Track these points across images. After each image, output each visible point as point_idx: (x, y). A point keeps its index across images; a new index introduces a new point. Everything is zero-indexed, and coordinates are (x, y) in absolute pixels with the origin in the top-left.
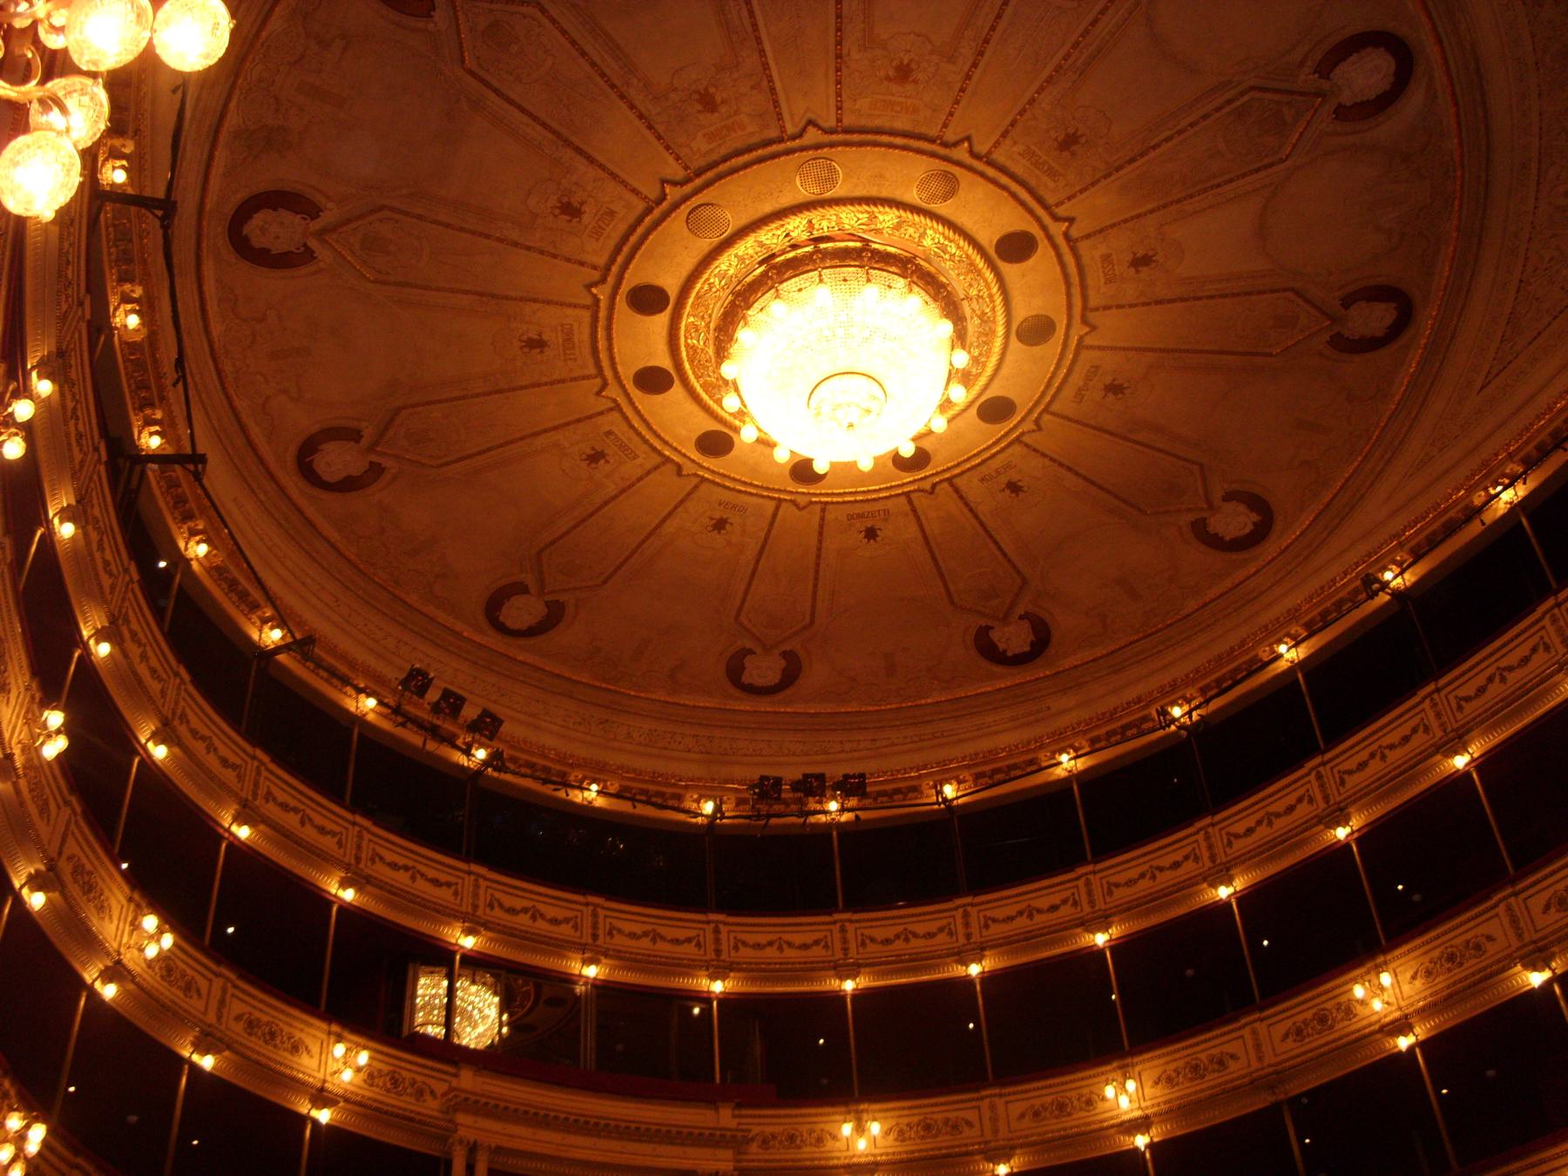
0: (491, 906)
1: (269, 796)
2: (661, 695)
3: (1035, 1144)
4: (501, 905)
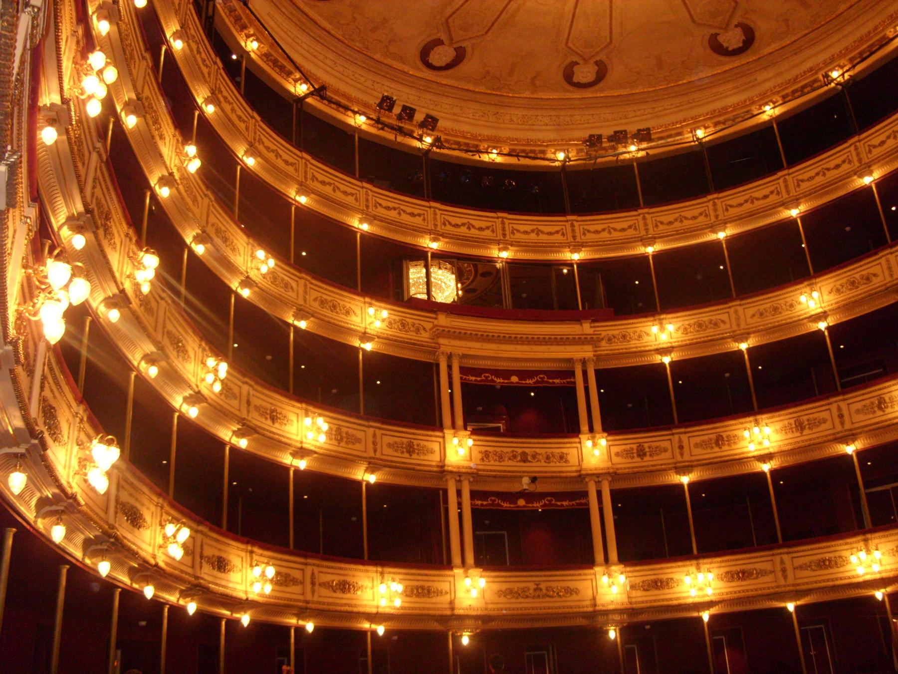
0: (445, 224)
1: (314, 178)
2: (527, 94)
3: (762, 330)
4: (450, 223)
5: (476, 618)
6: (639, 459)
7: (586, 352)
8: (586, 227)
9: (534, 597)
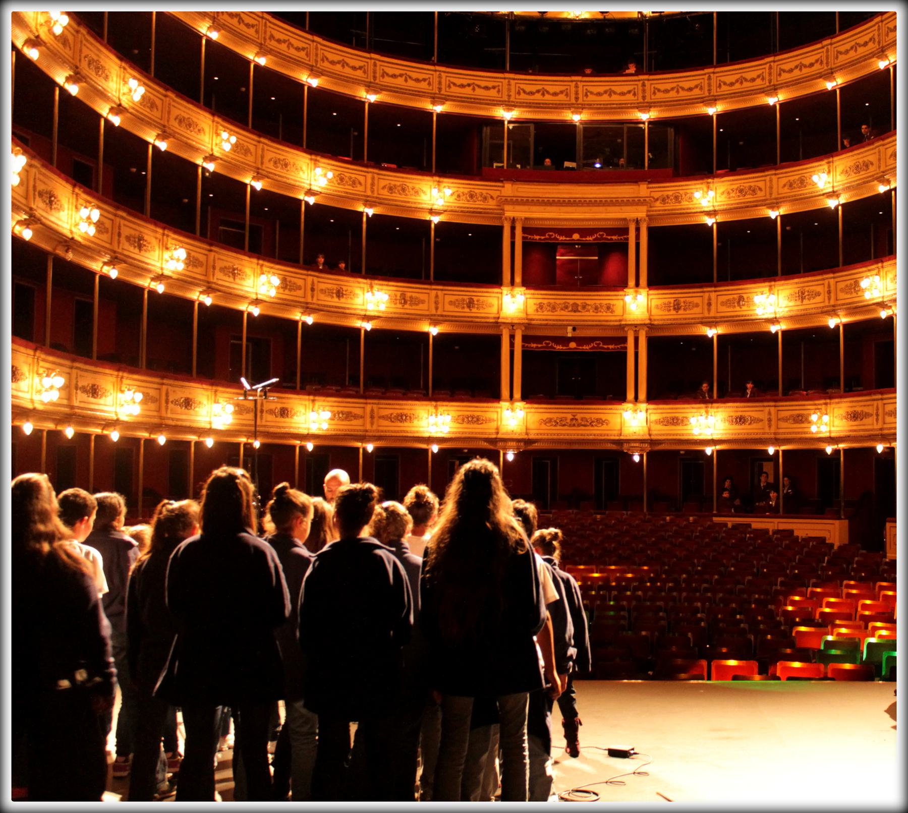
4: (524, 92)
5: (518, 441)
6: (674, 312)
7: (640, 213)
8: (657, 86)
9: (570, 426)
